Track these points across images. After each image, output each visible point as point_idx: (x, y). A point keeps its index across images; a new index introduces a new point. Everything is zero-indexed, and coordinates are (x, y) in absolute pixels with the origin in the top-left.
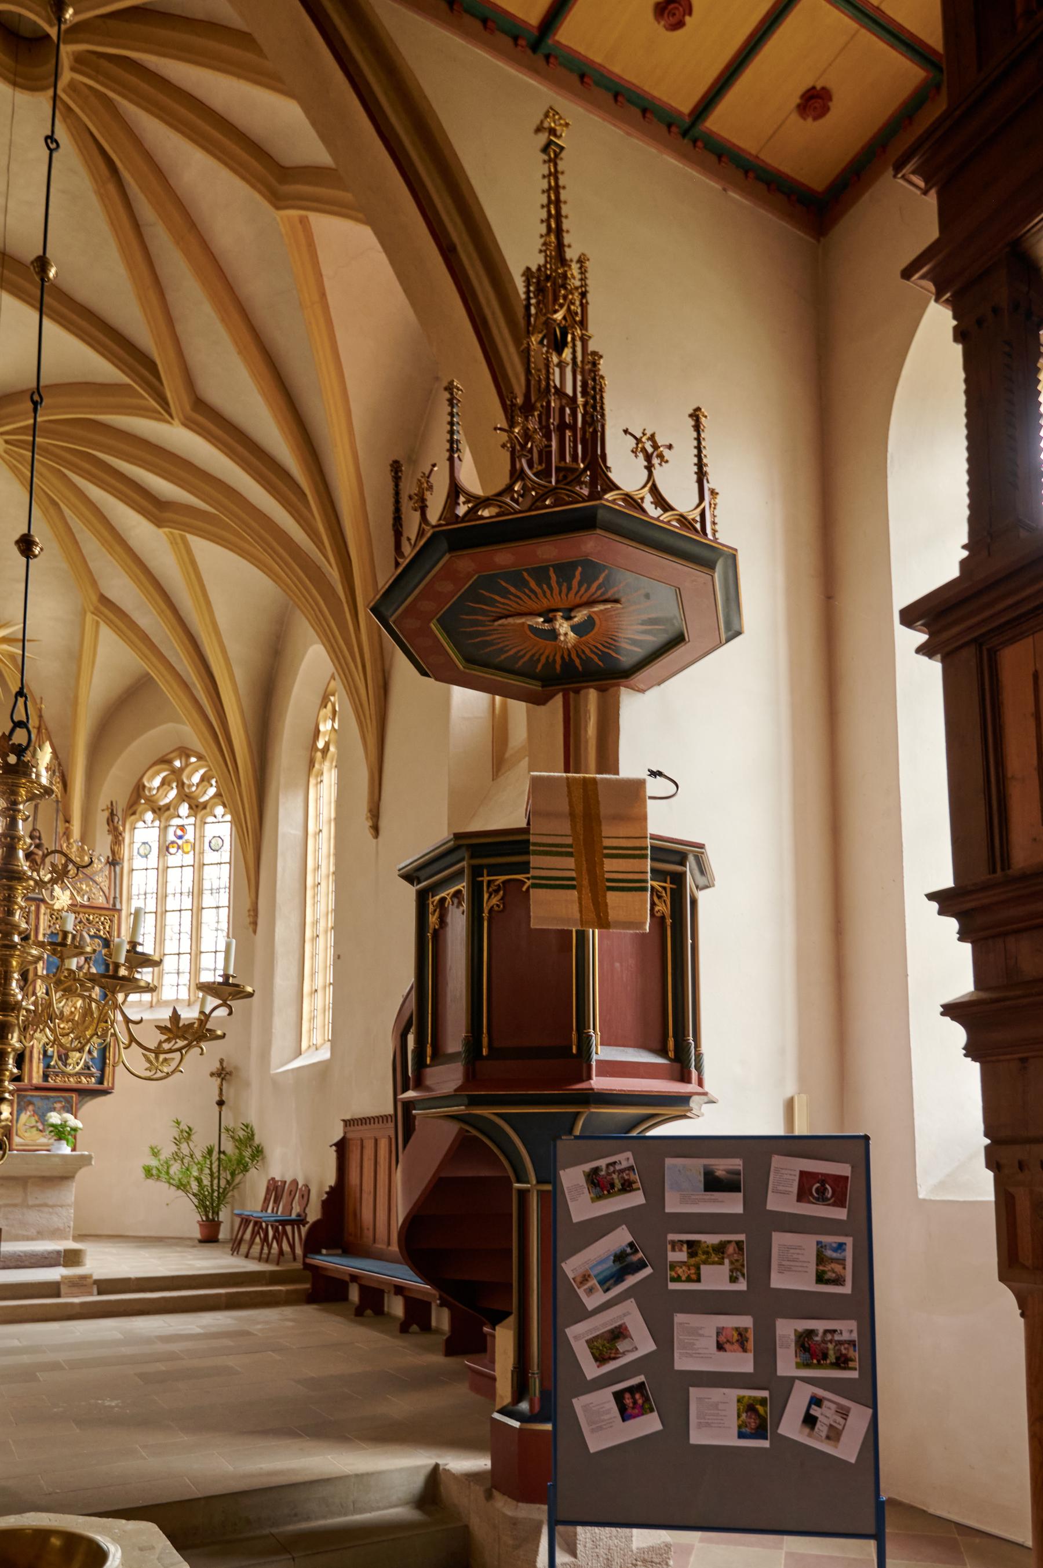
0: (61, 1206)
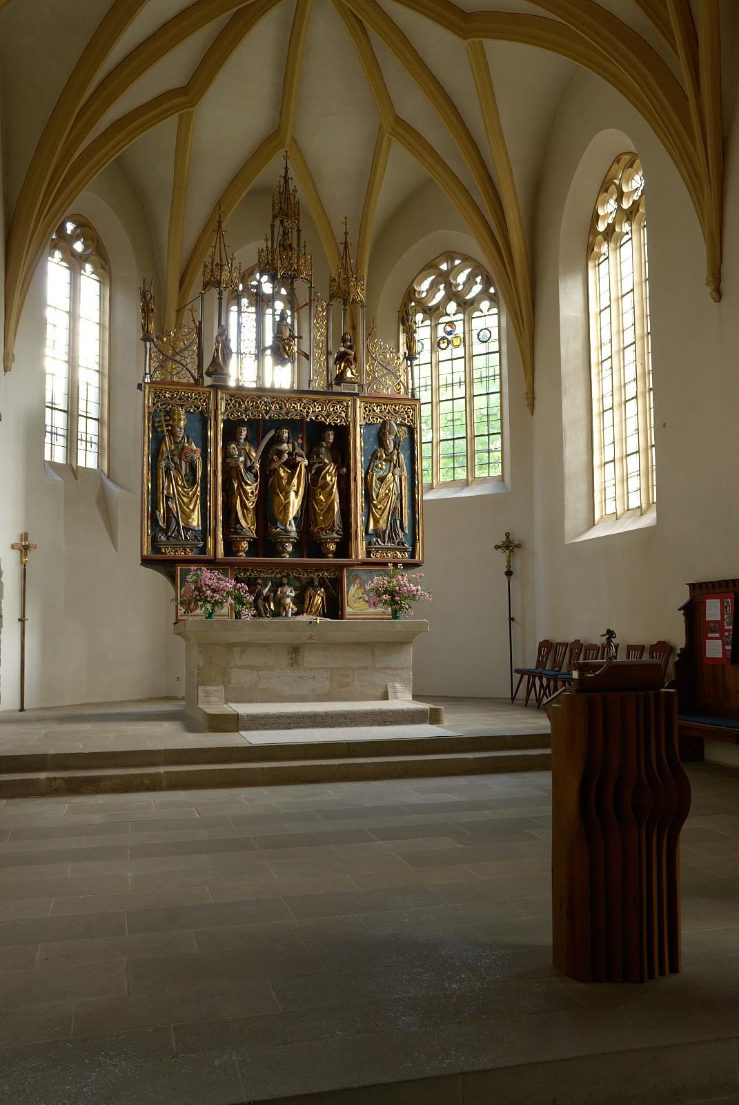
0: (403, 669)
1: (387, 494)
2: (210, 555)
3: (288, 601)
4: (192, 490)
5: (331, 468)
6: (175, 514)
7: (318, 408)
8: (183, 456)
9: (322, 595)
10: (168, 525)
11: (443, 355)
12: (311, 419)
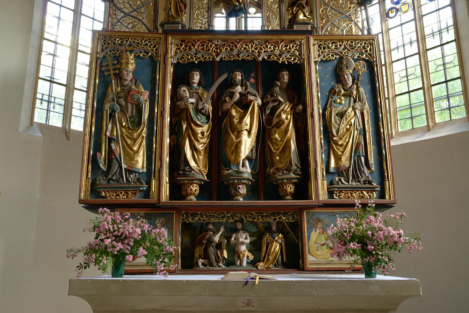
1: (348, 130)
2: (153, 199)
3: (243, 248)
4: (137, 132)
5: (287, 107)
6: (118, 157)
7: (270, 48)
8: (129, 98)
9: (280, 241)
10: (109, 167)
11: (391, 23)
12: (263, 59)
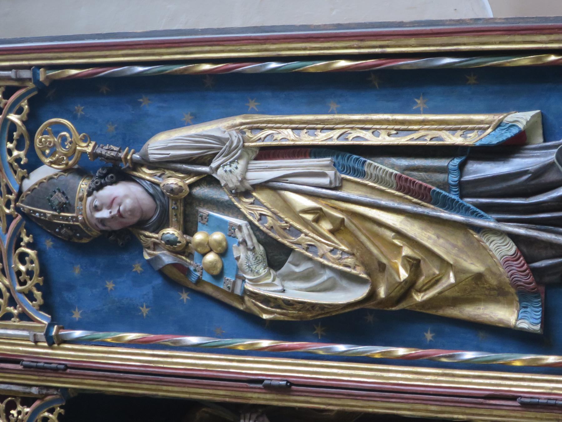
1: (339, 229)
